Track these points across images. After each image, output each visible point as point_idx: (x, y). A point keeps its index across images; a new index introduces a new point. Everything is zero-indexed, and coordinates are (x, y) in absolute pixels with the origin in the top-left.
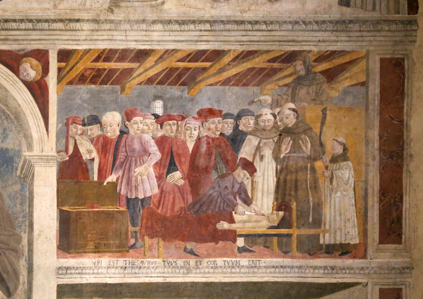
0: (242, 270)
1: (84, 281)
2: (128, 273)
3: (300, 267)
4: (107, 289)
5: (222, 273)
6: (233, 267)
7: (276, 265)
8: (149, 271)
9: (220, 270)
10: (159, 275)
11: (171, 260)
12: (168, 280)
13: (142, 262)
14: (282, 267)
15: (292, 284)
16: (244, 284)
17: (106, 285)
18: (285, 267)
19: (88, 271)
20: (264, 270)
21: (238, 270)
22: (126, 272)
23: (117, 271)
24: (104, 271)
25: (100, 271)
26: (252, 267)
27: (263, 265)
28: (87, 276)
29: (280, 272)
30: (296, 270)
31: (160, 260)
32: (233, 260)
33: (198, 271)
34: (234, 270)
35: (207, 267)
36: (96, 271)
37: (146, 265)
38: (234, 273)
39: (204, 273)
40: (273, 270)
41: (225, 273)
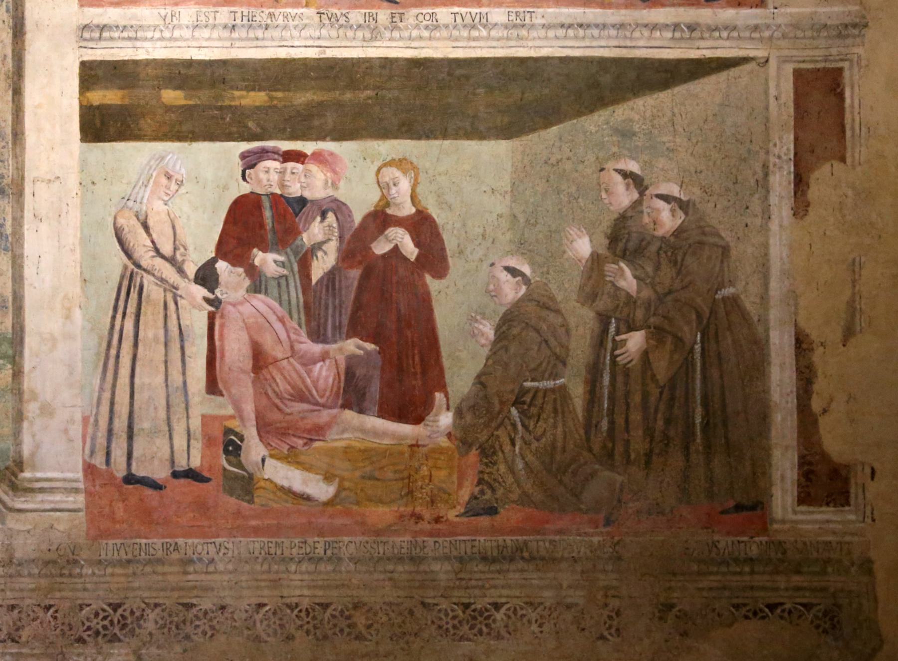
0: (493, 33)
1: (141, 55)
2: (241, 39)
3: (622, 26)
4: (192, 72)
5: (450, 38)
6: (473, 27)
7: (568, 21)
8: (286, 34)
9: (445, 33)
10: (310, 43)
11: (335, 11)
12: (330, 53)
13: (271, 15)
14: (581, 26)
15: (603, 63)
16: (497, 62)
17: (190, 63)
18: (589, 26)
19: (149, 34)
20: (542, 33)
21: (484, 33)
22: (235, 35)
23: (215, 35)
24: (187, 33)
25: (177, 33)
26: (515, 26)
27: (539, 21)
28: (147, 44)
29: (576, 37)
30: (613, 32)
31: (311, 12)
32: (474, 10)
33: (396, 34)
34: (475, 33)
35: (417, 27)
36: (167, 34)
37: (280, 21)
38: (475, 39)
39: (410, 38)
40: (561, 32)
41: (457, 39)
